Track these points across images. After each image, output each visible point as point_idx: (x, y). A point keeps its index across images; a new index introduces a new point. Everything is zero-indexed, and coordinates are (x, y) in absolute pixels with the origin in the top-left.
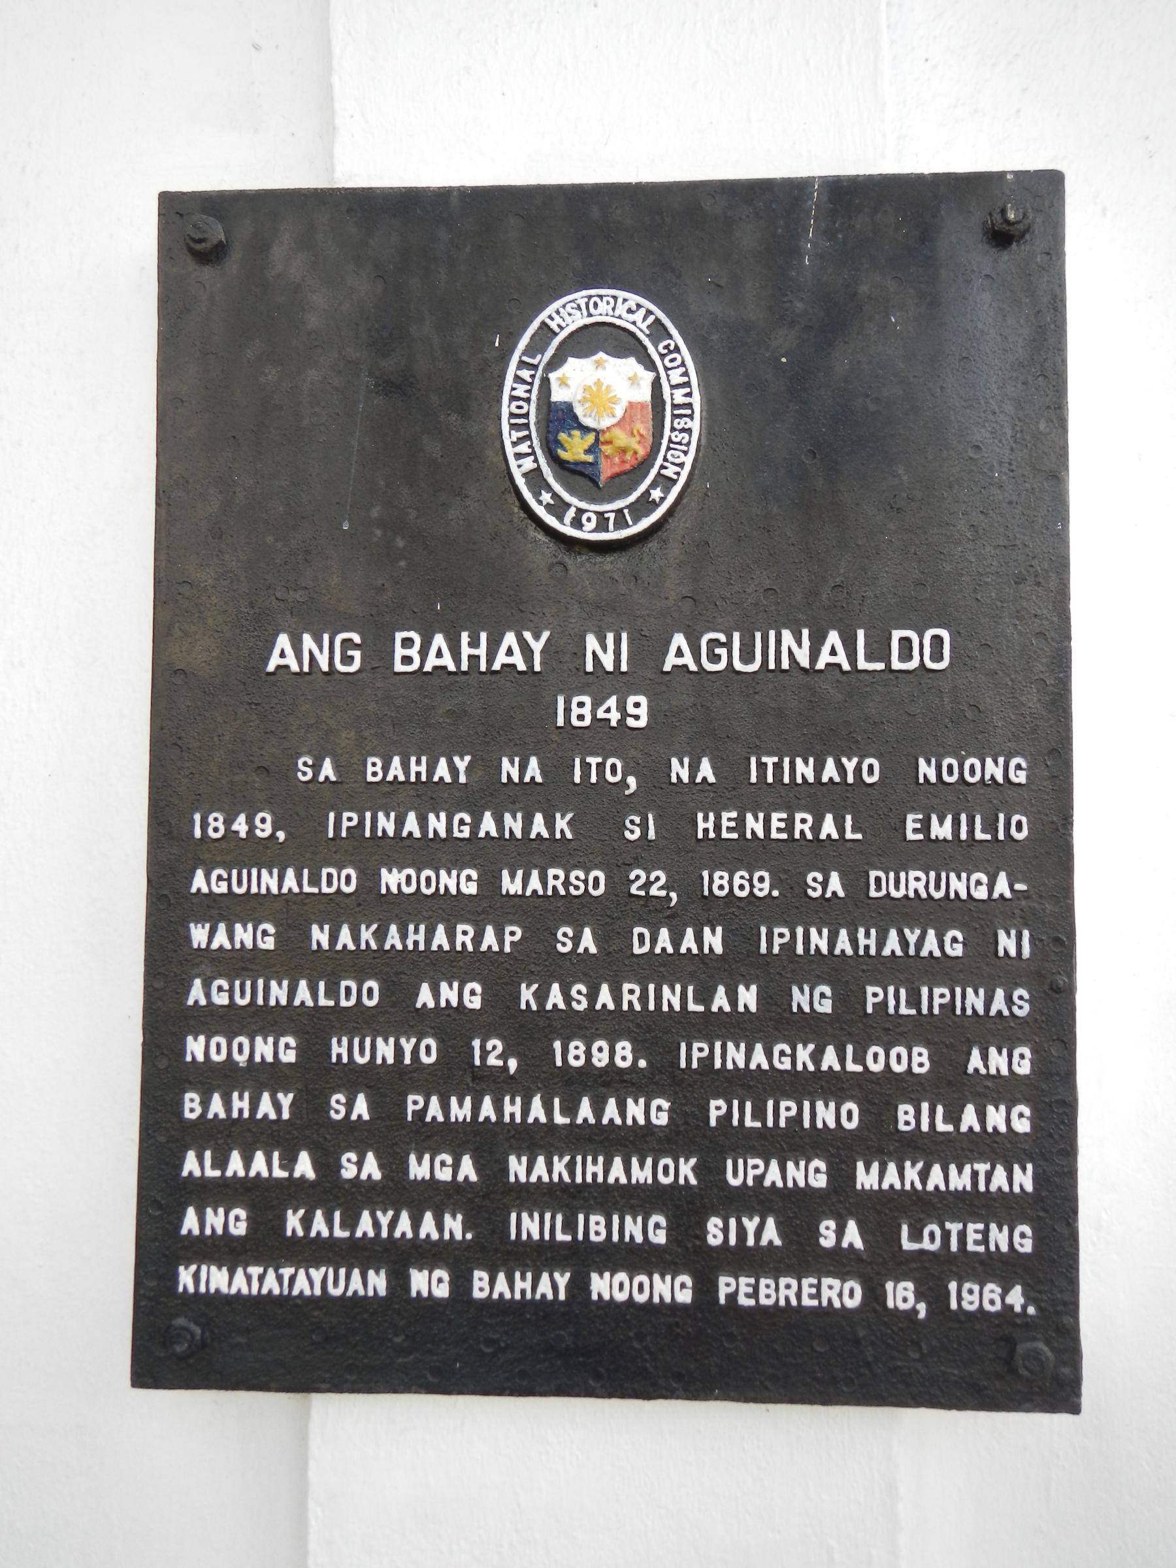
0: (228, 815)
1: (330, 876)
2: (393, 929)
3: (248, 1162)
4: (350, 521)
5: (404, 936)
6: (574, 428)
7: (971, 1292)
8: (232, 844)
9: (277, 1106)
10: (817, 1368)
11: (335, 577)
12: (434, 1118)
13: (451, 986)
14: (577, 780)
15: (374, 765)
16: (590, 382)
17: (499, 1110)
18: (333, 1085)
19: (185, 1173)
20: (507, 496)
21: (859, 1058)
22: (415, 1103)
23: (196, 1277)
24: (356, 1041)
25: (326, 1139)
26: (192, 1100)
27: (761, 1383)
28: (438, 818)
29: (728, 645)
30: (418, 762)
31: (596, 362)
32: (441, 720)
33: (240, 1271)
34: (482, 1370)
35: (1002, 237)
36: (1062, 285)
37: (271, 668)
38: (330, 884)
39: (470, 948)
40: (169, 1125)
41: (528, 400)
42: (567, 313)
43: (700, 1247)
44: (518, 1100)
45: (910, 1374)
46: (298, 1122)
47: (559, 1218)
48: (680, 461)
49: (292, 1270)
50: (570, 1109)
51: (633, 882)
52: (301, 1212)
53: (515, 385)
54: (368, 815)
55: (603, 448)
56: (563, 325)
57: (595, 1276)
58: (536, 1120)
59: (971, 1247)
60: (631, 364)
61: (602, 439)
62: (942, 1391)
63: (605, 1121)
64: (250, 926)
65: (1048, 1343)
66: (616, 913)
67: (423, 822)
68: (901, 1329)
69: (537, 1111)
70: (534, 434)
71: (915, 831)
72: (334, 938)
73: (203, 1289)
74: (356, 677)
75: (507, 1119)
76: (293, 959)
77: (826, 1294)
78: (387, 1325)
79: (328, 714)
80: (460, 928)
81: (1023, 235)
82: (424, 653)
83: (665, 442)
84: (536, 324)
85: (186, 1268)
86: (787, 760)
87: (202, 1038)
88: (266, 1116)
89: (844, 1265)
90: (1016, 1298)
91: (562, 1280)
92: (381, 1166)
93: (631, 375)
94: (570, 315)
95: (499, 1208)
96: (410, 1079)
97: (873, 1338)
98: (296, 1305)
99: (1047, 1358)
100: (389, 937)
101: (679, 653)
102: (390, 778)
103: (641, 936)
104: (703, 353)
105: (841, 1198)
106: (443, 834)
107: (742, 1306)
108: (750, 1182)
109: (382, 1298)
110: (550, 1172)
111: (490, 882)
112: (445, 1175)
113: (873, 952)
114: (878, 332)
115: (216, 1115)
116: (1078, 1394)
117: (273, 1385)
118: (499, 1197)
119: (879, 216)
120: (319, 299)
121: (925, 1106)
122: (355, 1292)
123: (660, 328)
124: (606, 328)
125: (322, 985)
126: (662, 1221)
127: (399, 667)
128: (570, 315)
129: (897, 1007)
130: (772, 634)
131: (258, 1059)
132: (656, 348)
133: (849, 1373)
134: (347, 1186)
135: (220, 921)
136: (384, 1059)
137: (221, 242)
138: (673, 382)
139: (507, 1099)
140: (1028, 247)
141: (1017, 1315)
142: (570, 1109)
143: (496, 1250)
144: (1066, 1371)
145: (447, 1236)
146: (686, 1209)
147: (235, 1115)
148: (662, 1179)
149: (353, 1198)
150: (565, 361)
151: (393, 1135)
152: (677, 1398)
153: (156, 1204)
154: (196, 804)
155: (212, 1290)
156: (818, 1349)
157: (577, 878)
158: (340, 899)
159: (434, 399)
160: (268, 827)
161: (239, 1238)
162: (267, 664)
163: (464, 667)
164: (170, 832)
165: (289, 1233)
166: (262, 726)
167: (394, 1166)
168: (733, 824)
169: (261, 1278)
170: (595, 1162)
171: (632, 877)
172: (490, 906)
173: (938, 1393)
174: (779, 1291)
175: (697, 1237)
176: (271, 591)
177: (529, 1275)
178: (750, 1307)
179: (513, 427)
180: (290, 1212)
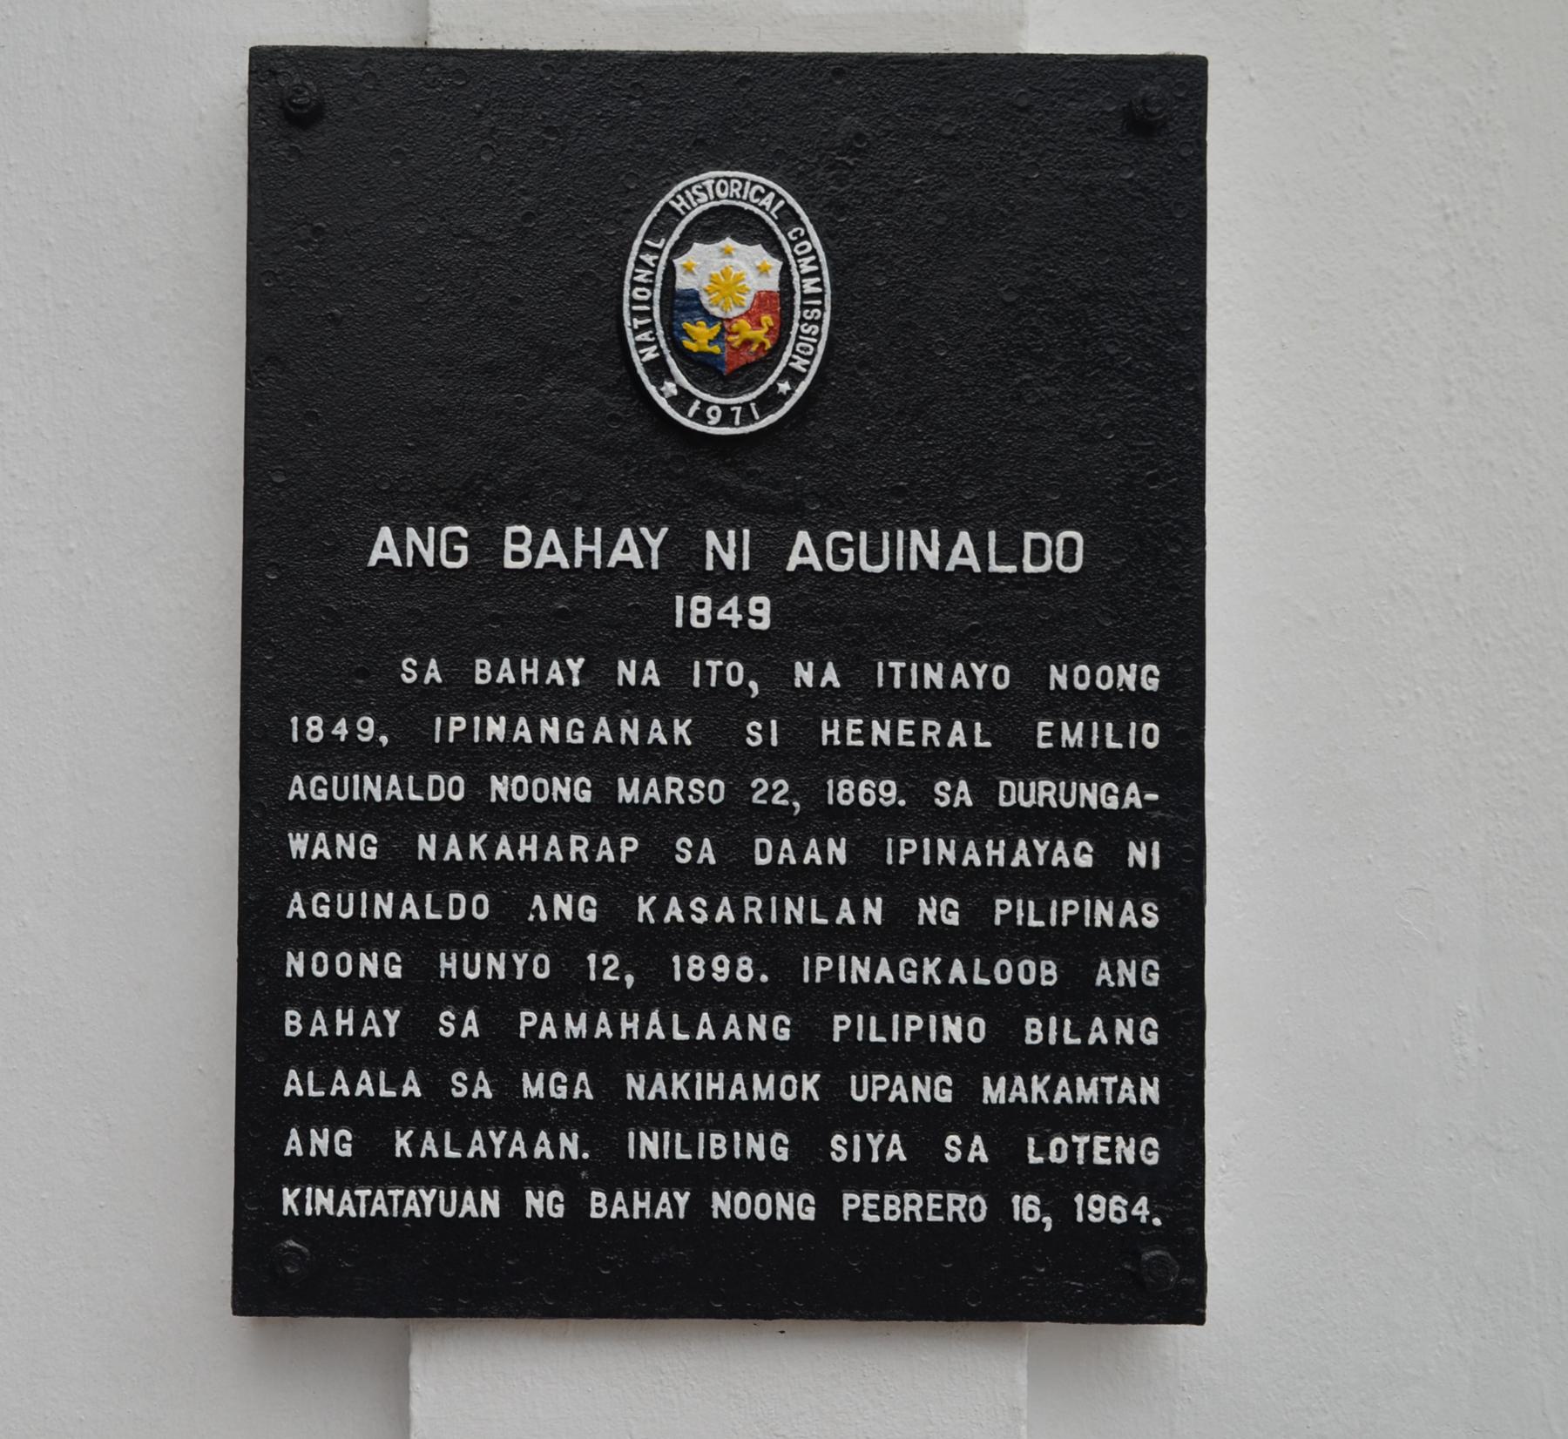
3: (352, 1082)
5: (515, 847)
14: (696, 684)
17: (615, 1026)
21: (987, 971)
29: (855, 545)
31: (722, 250)
38: (436, 792)
48: (807, 352)
50: (690, 1025)
51: (754, 791)
59: (1098, 1160)
66: (734, 823)
71: (1045, 739)
72: (441, 849)
76: (399, 870)
80: (574, 838)
82: (535, 549)
83: (793, 333)
86: (915, 665)
90: (1142, 1208)
91: (682, 1199)
101: (804, 552)
102: (500, 680)
103: (763, 846)
105: (967, 1113)
108: (875, 1098)
110: (669, 1090)
111: (606, 791)
113: (1001, 863)
121: (1053, 1020)
122: (468, 1214)
129: (1025, 919)
130: (900, 534)
138: (803, 271)
142: (690, 1025)
148: (784, 1096)
150: (690, 246)
151: (504, 1053)
157: (696, 786)
160: (371, 730)
163: (578, 563)
167: (507, 1084)
168: (858, 731)
169: (370, 1200)
170: (715, 1080)
171: (754, 784)
172: (604, 816)
174: (904, 1206)
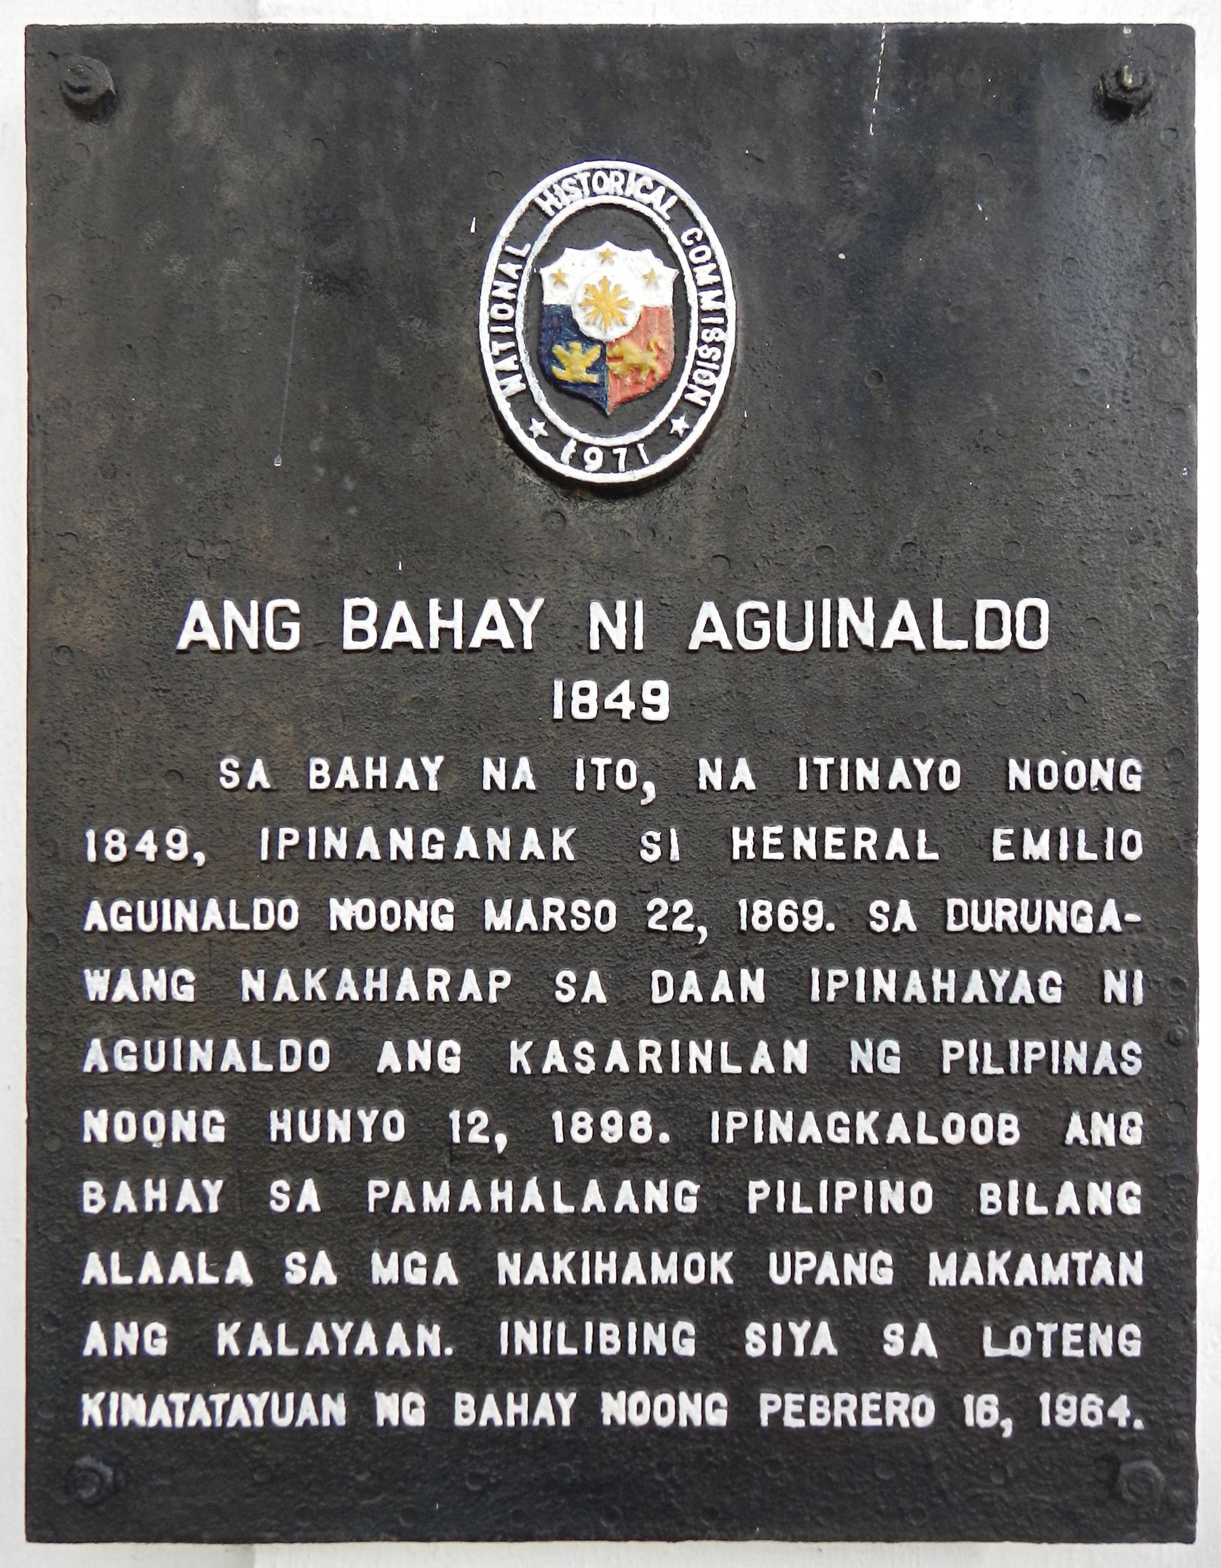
0: (131, 831)
1: (264, 908)
2: (347, 974)
3: (166, 1265)
4: (283, 456)
5: (360, 984)
6: (573, 339)
7: (1066, 1404)
8: (137, 870)
9: (203, 1197)
10: (880, 1499)
11: (264, 527)
12: (402, 1208)
13: (421, 1046)
14: (580, 786)
15: (319, 767)
16: (594, 281)
17: (485, 1197)
18: (272, 1169)
19: (86, 1281)
20: (487, 425)
21: (934, 1128)
22: (378, 1190)
23: (105, 1407)
24: (302, 1114)
25: (265, 1236)
26: (93, 1190)
27: (812, 1518)
28: (402, 834)
29: (771, 617)
30: (376, 765)
31: (602, 254)
32: (405, 711)
33: (160, 1399)
34: (467, 1512)
35: (1117, 107)
36: (1191, 170)
37: (183, 644)
38: (264, 918)
39: (445, 997)
40: (63, 1221)
41: (514, 303)
42: (564, 191)
43: (737, 1359)
44: (509, 1184)
45: (993, 1503)
46: (230, 1215)
47: (562, 1327)
48: (709, 384)
49: (226, 1397)
50: (575, 1194)
51: (652, 913)
52: (236, 1326)
53: (497, 283)
54: (312, 831)
55: (611, 365)
56: (559, 206)
57: (606, 1397)
58: (532, 1208)
59: (1067, 1352)
60: (646, 259)
61: (609, 353)
62: (1030, 1521)
63: (618, 1209)
64: (162, 973)
65: (1157, 1462)
66: (630, 953)
67: (383, 840)
68: (982, 1450)
69: (533, 1197)
70: (522, 347)
71: (1004, 849)
72: (270, 986)
73: (113, 1421)
74: (294, 656)
75: (495, 1208)
76: (219, 1013)
77: (891, 1411)
78: (347, 1460)
79: (259, 703)
80: (432, 972)
81: (1142, 106)
82: (381, 626)
83: (690, 359)
84: (523, 205)
85: (92, 1396)
86: (845, 762)
87: (103, 1113)
88: (188, 1208)
89: (913, 1377)
90: (1121, 1410)
91: (566, 1402)
92: (336, 1268)
93: (647, 272)
94: (567, 193)
95: (486, 1317)
96: (371, 1160)
97: (948, 1462)
98: (233, 1439)
99: (1157, 1480)
100: (342, 984)
101: (709, 627)
102: (340, 784)
103: (662, 981)
104: (739, 246)
105: (911, 1297)
106: (409, 855)
107: (789, 1428)
108: (799, 1280)
109: (341, 1428)
110: (550, 1271)
111: (469, 915)
112: (417, 1278)
113: (951, 998)
114: (961, 223)
115: (124, 1208)
116: (1193, 1521)
117: (205, 1535)
118: (485, 1303)
119: (963, 75)
120: (239, 168)
121: (1014, 1185)
122: (307, 1422)
123: (684, 212)
124: (615, 211)
125: (256, 1045)
126: (690, 1328)
127: (349, 644)
128: (567, 193)
129: (980, 1065)
130: (827, 603)
131: (176, 1138)
132: (679, 238)
133: (918, 1504)
134: (293, 1293)
135: (123, 966)
136: (337, 1136)
137: (109, 91)
138: (701, 283)
139: (495, 1183)
140: (1148, 121)
141: (1122, 1430)
142: (575, 1194)
143: (483, 1368)
144: (1178, 1493)
145: (421, 1352)
146: (718, 1313)
147: (149, 1207)
148: (690, 1278)
149: (305, 1306)
150: (562, 253)
151: (351, 1229)
152: (710, 1539)
153: (50, 1318)
154: (90, 818)
155: (125, 1423)
156: (882, 1477)
157: (581, 909)
158: (277, 937)
159: (392, 298)
160: (183, 847)
161: (158, 1358)
162: (177, 640)
163: (434, 643)
164: (56, 854)
165: (221, 1352)
166: (172, 719)
167: (353, 1267)
168: (777, 841)
169: (187, 1407)
170: (606, 1258)
171: (650, 907)
172: (469, 946)
173: (1026, 1524)
174: (832, 1410)
175: (733, 1347)
176: (182, 546)
177: (525, 1397)
178: (798, 1429)
179: (494, 336)
180: (222, 1326)
